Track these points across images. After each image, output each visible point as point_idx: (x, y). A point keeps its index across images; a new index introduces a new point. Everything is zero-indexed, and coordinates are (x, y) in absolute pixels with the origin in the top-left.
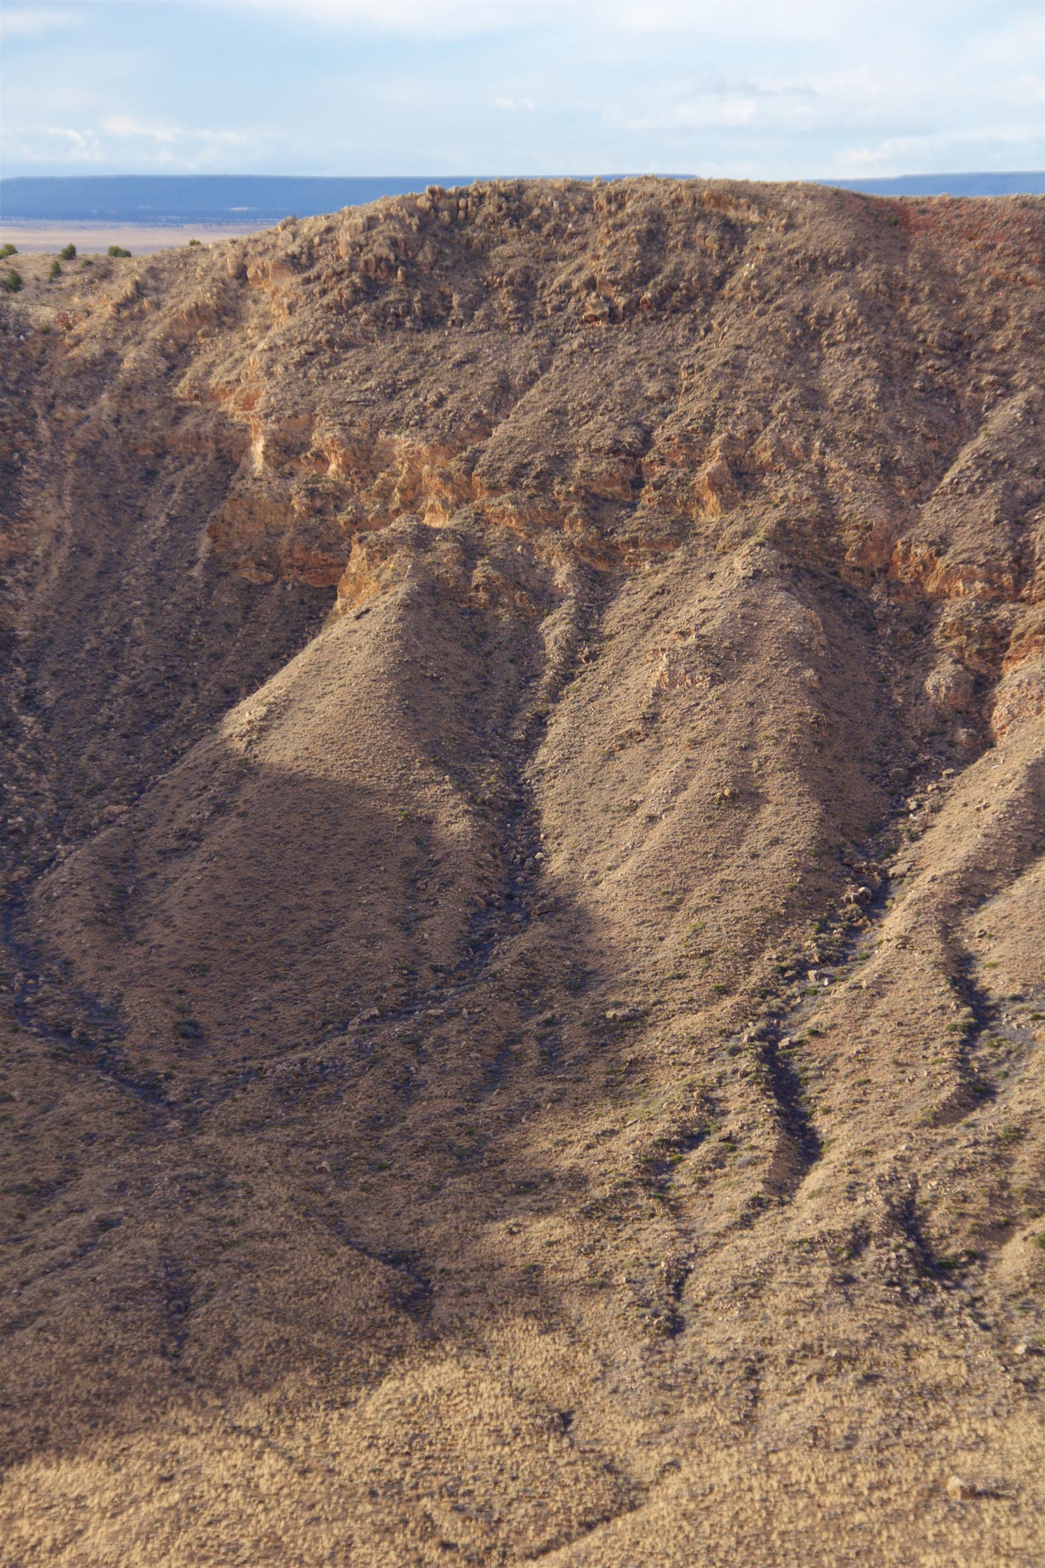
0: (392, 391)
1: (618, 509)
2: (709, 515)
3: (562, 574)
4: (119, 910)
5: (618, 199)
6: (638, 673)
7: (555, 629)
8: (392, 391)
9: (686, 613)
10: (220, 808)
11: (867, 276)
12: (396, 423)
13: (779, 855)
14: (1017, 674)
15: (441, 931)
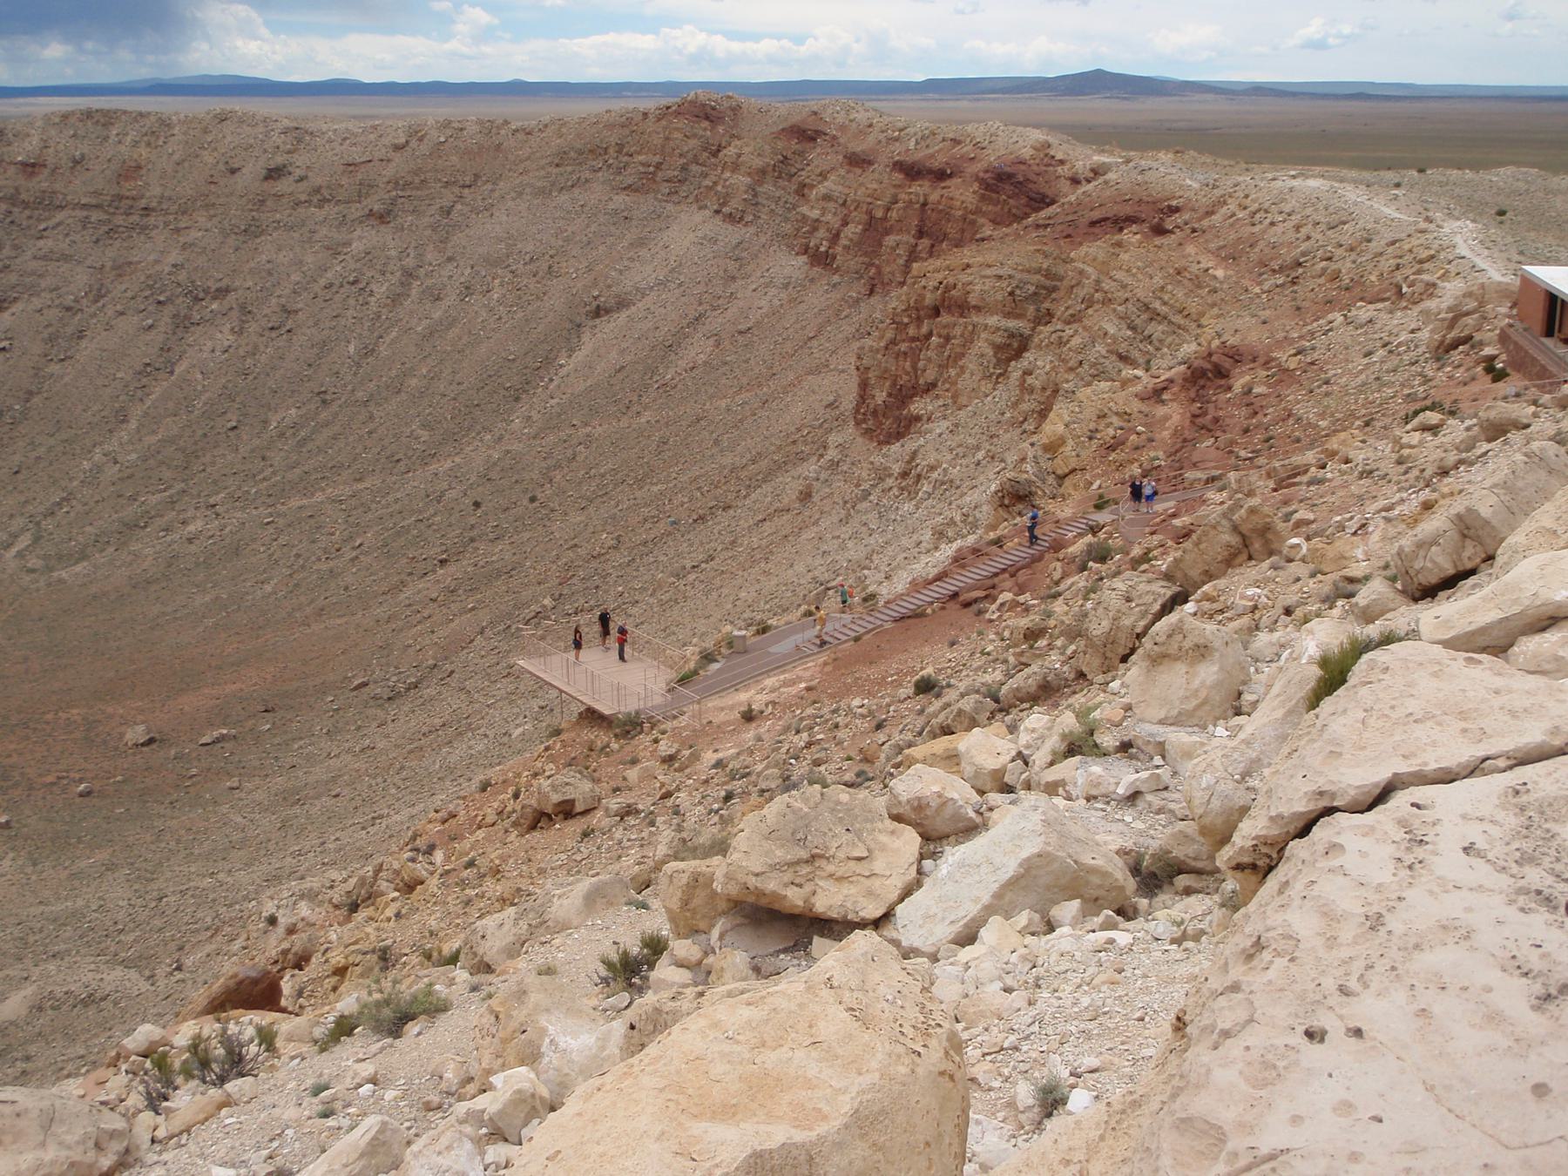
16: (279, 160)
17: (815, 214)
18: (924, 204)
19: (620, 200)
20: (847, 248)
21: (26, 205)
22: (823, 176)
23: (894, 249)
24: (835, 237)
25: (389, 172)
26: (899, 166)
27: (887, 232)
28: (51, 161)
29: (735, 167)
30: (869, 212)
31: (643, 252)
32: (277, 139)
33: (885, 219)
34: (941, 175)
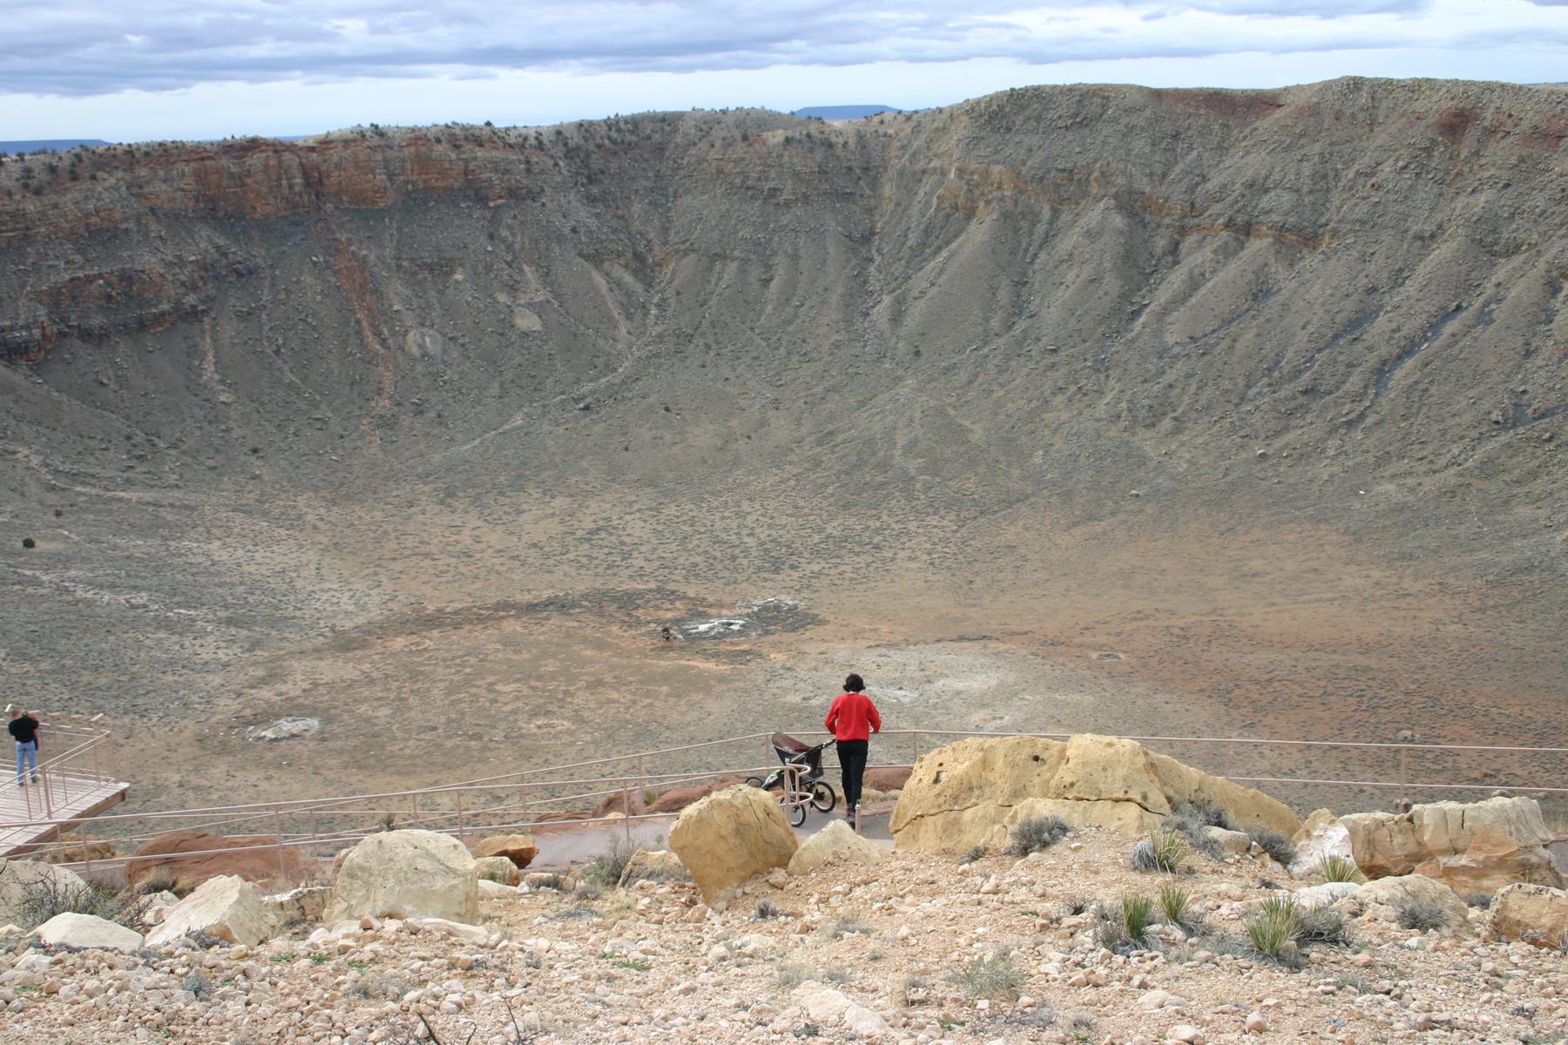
0: (996, 152)
1: (1068, 188)
2: (1094, 189)
3: (1046, 213)
4: (896, 318)
5: (1071, 89)
6: (1069, 241)
7: (1041, 229)
8: (996, 152)
9: (1083, 222)
10: (933, 284)
11: (1148, 113)
12: (997, 162)
13: (1107, 298)
14: (1190, 240)
15: (995, 323)
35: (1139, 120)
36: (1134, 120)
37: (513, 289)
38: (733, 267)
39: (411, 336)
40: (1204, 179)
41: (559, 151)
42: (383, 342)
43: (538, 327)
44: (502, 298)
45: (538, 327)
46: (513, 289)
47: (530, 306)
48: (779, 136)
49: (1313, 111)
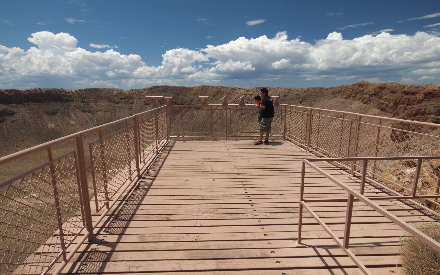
16: (286, 94)
17: (383, 102)
18: (409, 99)
19: (343, 100)
20: (389, 108)
21: (250, 100)
22: (385, 95)
23: (401, 108)
24: (387, 106)
25: (303, 96)
26: (403, 92)
27: (399, 105)
28: (254, 94)
29: (366, 94)
30: (395, 101)
31: (346, 109)
32: (286, 91)
33: (399, 102)
34: (414, 94)
35: (173, 91)
36: (172, 91)
37: (69, 117)
38: (109, 113)
39: (49, 125)
40: (183, 100)
41: (76, 93)
42: (43, 126)
43: (74, 123)
44: (67, 118)
45: (74, 123)
46: (69, 117)
47: (73, 120)
48: (116, 92)
49: (198, 90)
